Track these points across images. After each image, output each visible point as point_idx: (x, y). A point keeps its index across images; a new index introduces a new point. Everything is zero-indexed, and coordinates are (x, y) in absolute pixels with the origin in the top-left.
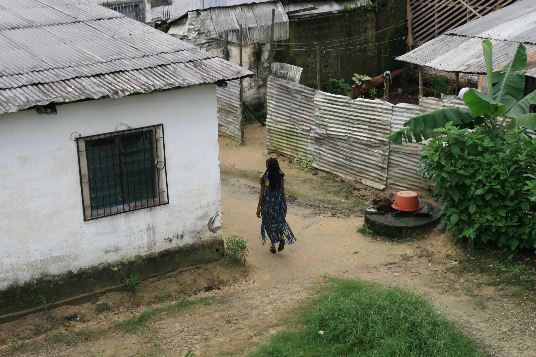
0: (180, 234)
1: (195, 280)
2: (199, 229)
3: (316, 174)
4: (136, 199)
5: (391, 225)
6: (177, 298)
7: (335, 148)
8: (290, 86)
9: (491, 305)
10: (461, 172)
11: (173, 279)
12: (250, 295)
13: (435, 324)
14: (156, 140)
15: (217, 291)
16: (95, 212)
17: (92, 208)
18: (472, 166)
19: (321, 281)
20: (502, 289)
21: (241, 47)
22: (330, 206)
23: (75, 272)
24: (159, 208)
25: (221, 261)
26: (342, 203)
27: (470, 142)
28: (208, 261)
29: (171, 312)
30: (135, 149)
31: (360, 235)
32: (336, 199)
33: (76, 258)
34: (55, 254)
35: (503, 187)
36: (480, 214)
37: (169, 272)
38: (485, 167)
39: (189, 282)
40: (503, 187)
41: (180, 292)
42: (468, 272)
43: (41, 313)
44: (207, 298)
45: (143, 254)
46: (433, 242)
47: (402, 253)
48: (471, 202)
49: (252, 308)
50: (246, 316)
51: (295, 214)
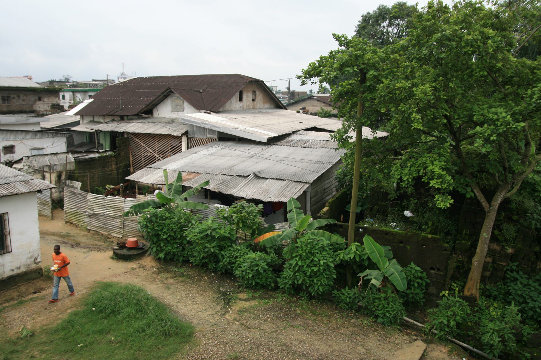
3: (89, 232)
7: (98, 219)
8: (75, 191)
9: (172, 287)
10: (156, 228)
13: (148, 299)
15: (39, 293)
18: (161, 226)
20: (177, 280)
21: (50, 173)
22: (96, 247)
25: (41, 278)
26: (102, 245)
27: (160, 215)
28: (34, 279)
31: (111, 260)
32: (99, 243)
35: (175, 234)
38: (167, 226)
40: (175, 234)
42: (161, 273)
44: (34, 298)
46: (145, 260)
48: (162, 241)
51: (79, 252)
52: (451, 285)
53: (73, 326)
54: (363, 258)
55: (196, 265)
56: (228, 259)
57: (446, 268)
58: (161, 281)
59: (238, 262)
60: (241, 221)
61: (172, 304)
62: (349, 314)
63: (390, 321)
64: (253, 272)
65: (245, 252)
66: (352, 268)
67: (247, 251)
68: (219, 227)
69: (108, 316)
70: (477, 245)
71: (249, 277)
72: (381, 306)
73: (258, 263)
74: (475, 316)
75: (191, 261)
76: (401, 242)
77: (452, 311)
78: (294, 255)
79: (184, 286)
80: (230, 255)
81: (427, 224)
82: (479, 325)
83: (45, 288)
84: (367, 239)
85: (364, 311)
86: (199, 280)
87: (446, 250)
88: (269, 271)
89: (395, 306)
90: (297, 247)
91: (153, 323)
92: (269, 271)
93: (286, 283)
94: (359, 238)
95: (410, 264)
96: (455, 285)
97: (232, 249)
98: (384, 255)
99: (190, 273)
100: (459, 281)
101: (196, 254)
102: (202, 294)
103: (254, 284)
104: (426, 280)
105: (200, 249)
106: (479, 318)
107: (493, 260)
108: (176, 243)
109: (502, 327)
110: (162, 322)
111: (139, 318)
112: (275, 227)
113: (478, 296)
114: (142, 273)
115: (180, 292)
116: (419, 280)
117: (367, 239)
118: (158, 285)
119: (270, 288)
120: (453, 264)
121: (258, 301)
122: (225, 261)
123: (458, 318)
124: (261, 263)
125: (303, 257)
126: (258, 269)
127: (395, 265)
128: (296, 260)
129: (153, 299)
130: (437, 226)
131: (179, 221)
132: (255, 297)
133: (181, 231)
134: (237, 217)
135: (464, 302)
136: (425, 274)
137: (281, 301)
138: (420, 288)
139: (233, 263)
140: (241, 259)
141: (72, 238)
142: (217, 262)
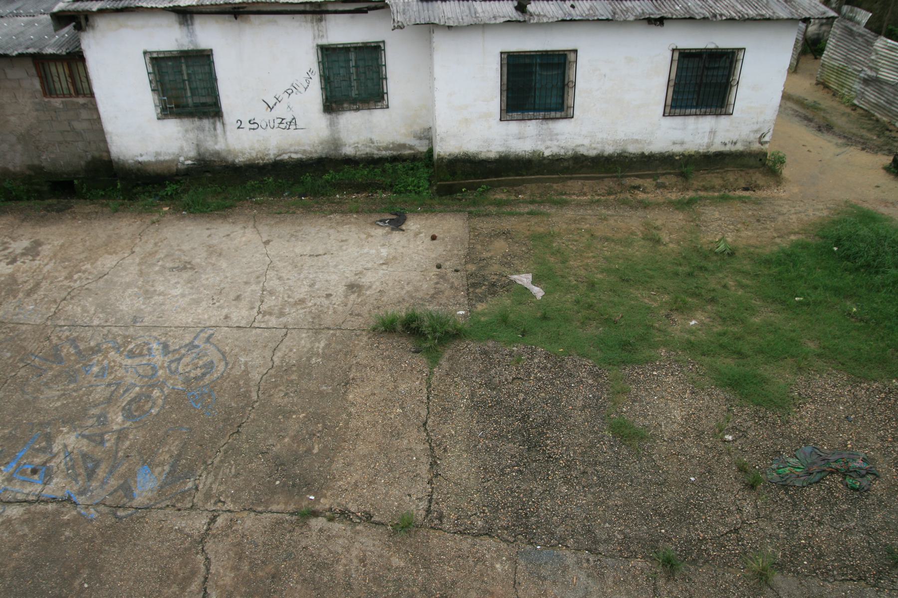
0: (734, 141)
1: (736, 180)
2: (750, 140)
4: (707, 107)
6: (719, 191)
11: (720, 175)
12: (780, 202)
14: (736, 61)
15: (752, 192)
16: (673, 110)
17: (672, 107)
19: (843, 204)
23: (647, 154)
24: (723, 117)
25: (761, 169)
28: (751, 167)
29: (714, 201)
30: (717, 65)
33: (650, 143)
34: (636, 137)
37: (717, 169)
39: (732, 180)
41: (723, 186)
43: (615, 179)
44: (744, 197)
45: (701, 151)
49: (780, 214)
50: (773, 220)
51: (830, 142)
53: (795, 265)
83: (763, 186)
141: (822, 114)
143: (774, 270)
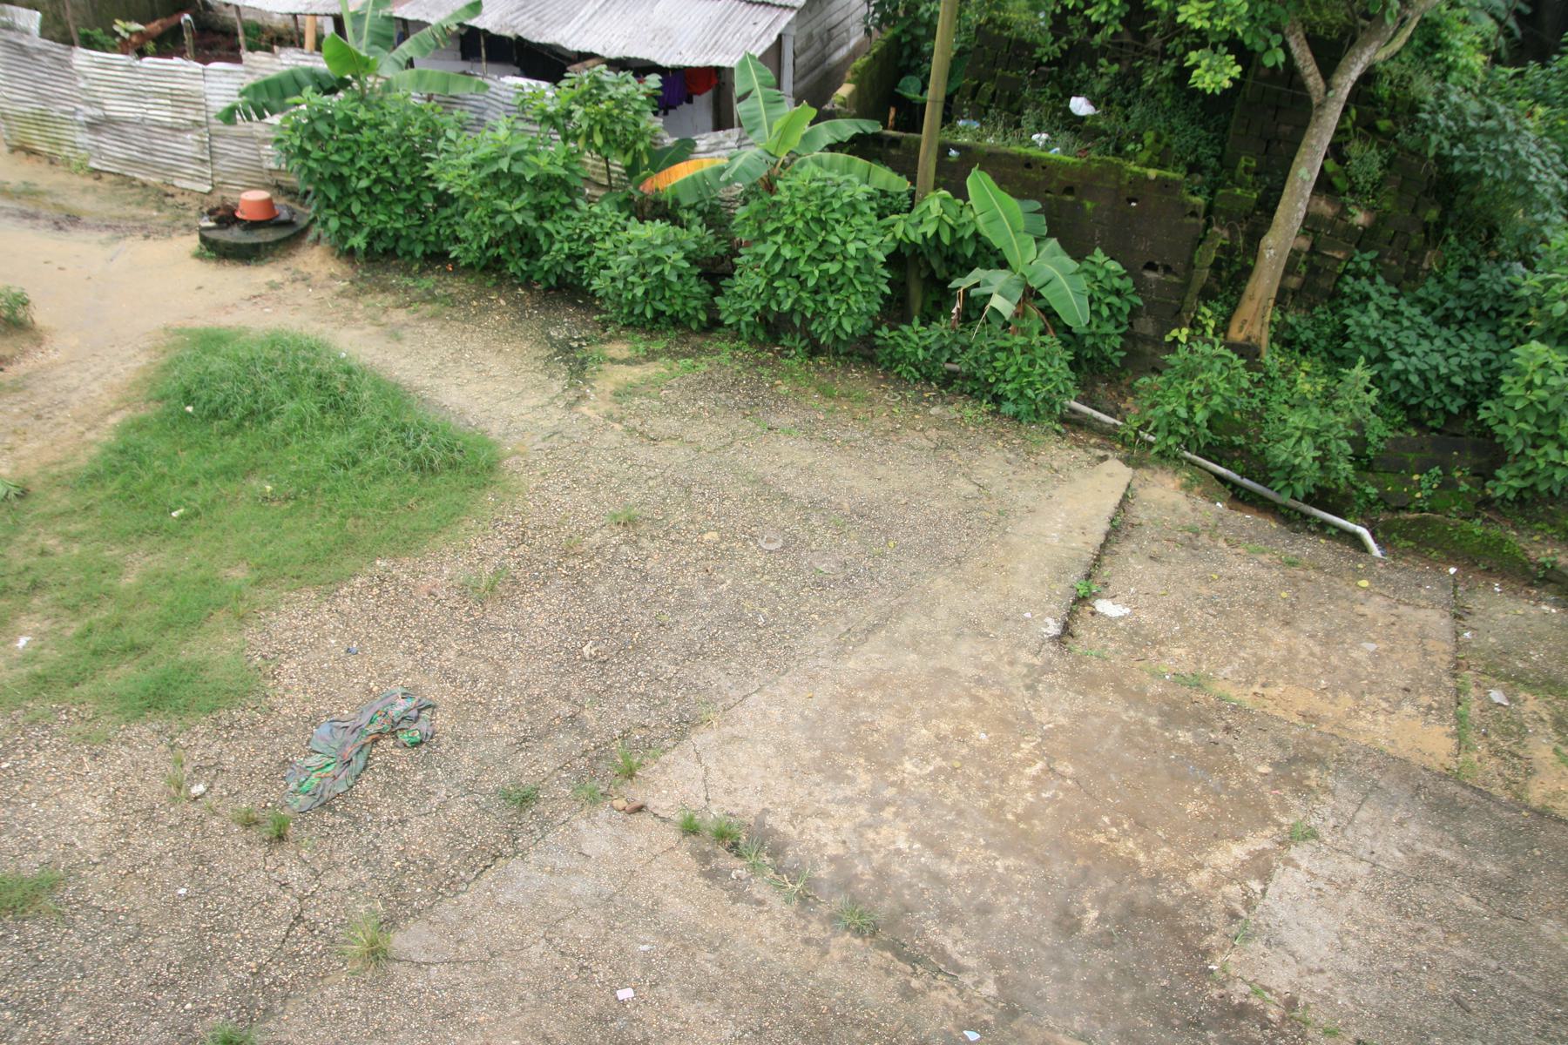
3: (99, 178)
5: (242, 241)
7: (122, 136)
9: (407, 333)
10: (335, 158)
13: (349, 372)
18: (349, 148)
19: (163, 335)
20: (416, 311)
22: (137, 224)
26: (153, 218)
27: (339, 115)
31: (198, 261)
32: (142, 212)
35: (395, 174)
36: (368, 213)
38: (365, 147)
40: (395, 174)
42: (365, 293)
46: (306, 258)
47: (267, 280)
48: (353, 199)
52: (1197, 313)
53: (141, 463)
54: (959, 235)
55: (470, 266)
56: (566, 246)
57: (1190, 266)
58: (369, 317)
59: (598, 253)
60: (598, 128)
61: (417, 383)
62: (923, 392)
63: (1036, 410)
64: (647, 280)
65: (616, 223)
66: (928, 264)
67: (621, 221)
68: (532, 147)
69: (239, 426)
70: (1277, 204)
71: (634, 296)
72: (1013, 369)
73: (661, 253)
74: (1252, 396)
75: (452, 256)
76: (1069, 190)
77: (1201, 382)
78: (769, 227)
79: (442, 328)
80: (570, 232)
81: (1139, 138)
82: (1261, 418)
84: (979, 182)
85: (962, 386)
86: (484, 311)
87: (1194, 214)
88: (692, 275)
89: (1051, 370)
90: (775, 204)
91: (377, 438)
92: (692, 275)
93: (742, 312)
94: (952, 178)
95: (1091, 253)
96: (1208, 313)
97: (576, 215)
98: (1021, 225)
99: (450, 290)
100: (1217, 301)
101: (465, 233)
102: (500, 351)
103: (649, 314)
104: (1130, 297)
105: (480, 217)
106: (1263, 401)
107: (1313, 246)
108: (401, 201)
109: (1325, 421)
110: (404, 435)
111: (333, 427)
112: (695, 145)
113: (1265, 342)
114: (302, 294)
115: (433, 347)
116: (1113, 299)
117: (979, 182)
118: (362, 328)
119: (694, 326)
120: (1207, 256)
121: (664, 362)
122: (558, 251)
123: (1217, 400)
124: (670, 254)
125: (796, 232)
126: (661, 273)
127: (1054, 255)
128: (775, 243)
129: (364, 371)
130: (1168, 146)
131: (405, 132)
132: (653, 351)
133: (413, 164)
134: (586, 114)
135: (1235, 357)
136: (1128, 283)
137: (731, 361)
138: (1113, 321)
139: (581, 257)
140: (608, 245)
142: (533, 253)
143: (113, 486)
